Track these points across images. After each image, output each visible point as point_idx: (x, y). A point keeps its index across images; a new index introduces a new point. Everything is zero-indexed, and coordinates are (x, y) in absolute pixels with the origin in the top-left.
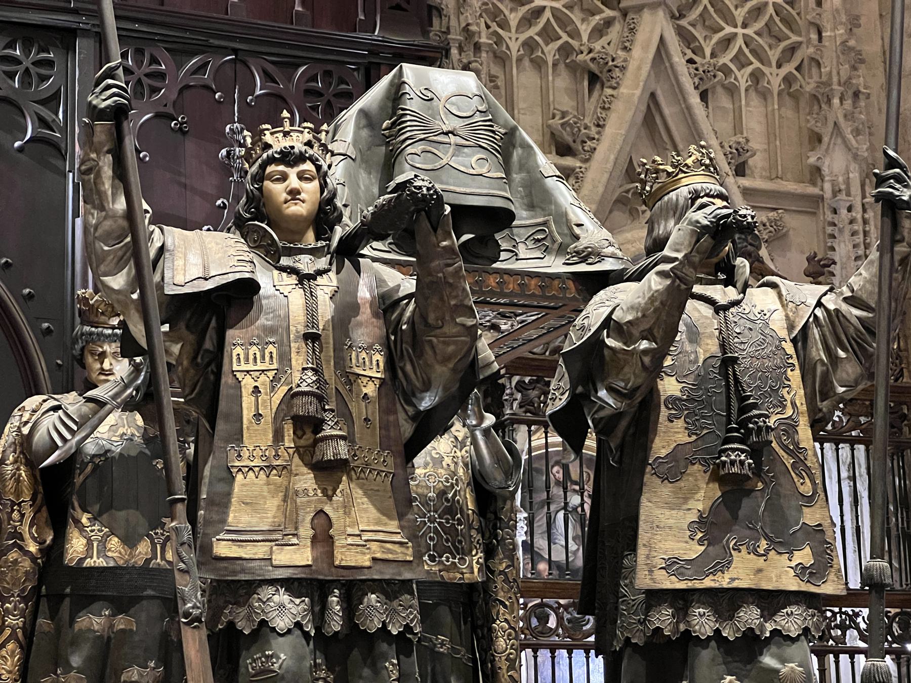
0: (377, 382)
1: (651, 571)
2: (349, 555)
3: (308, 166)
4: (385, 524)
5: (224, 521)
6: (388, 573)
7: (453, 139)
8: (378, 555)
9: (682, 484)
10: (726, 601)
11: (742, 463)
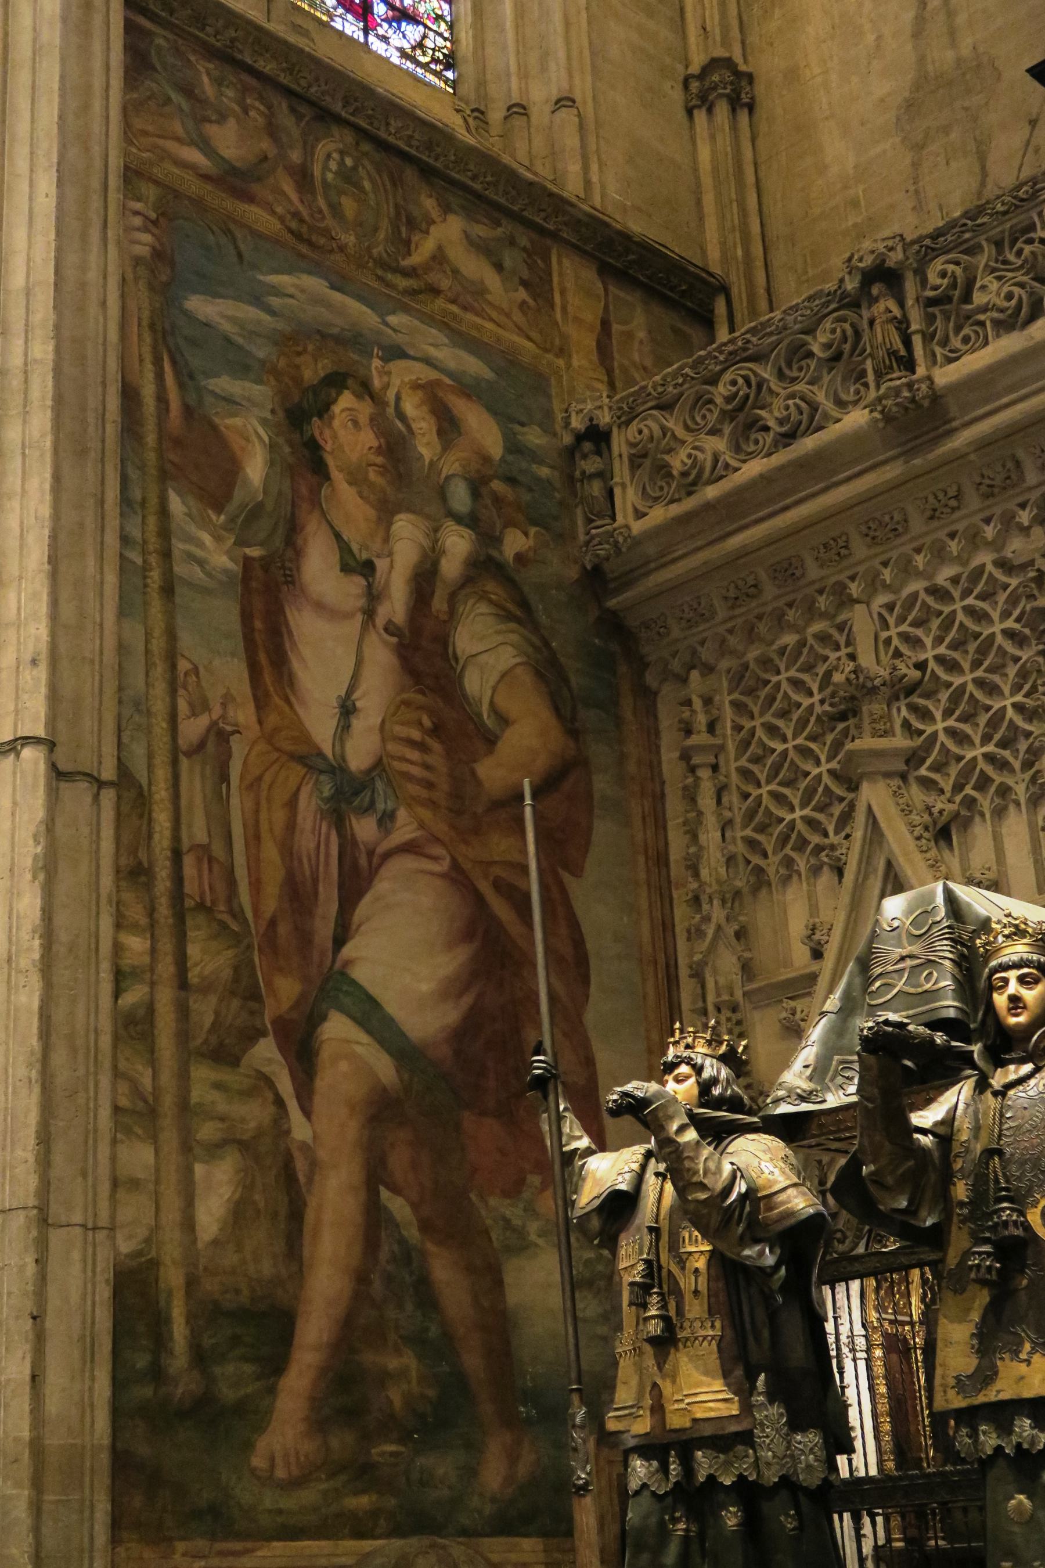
0: (707, 1255)
1: (945, 1392)
2: (675, 1421)
3: (684, 1069)
4: (709, 1385)
5: (612, 1401)
6: (708, 1431)
7: (909, 963)
8: (699, 1415)
9: (965, 1295)
10: (1002, 1413)
11: (978, 1266)
